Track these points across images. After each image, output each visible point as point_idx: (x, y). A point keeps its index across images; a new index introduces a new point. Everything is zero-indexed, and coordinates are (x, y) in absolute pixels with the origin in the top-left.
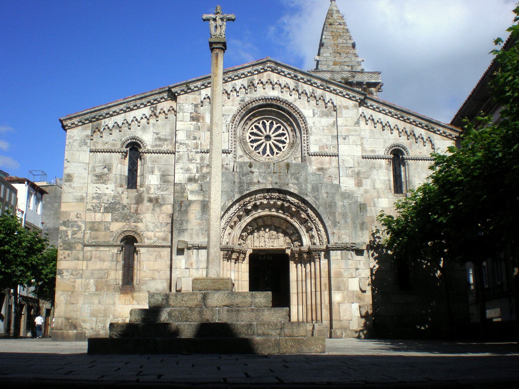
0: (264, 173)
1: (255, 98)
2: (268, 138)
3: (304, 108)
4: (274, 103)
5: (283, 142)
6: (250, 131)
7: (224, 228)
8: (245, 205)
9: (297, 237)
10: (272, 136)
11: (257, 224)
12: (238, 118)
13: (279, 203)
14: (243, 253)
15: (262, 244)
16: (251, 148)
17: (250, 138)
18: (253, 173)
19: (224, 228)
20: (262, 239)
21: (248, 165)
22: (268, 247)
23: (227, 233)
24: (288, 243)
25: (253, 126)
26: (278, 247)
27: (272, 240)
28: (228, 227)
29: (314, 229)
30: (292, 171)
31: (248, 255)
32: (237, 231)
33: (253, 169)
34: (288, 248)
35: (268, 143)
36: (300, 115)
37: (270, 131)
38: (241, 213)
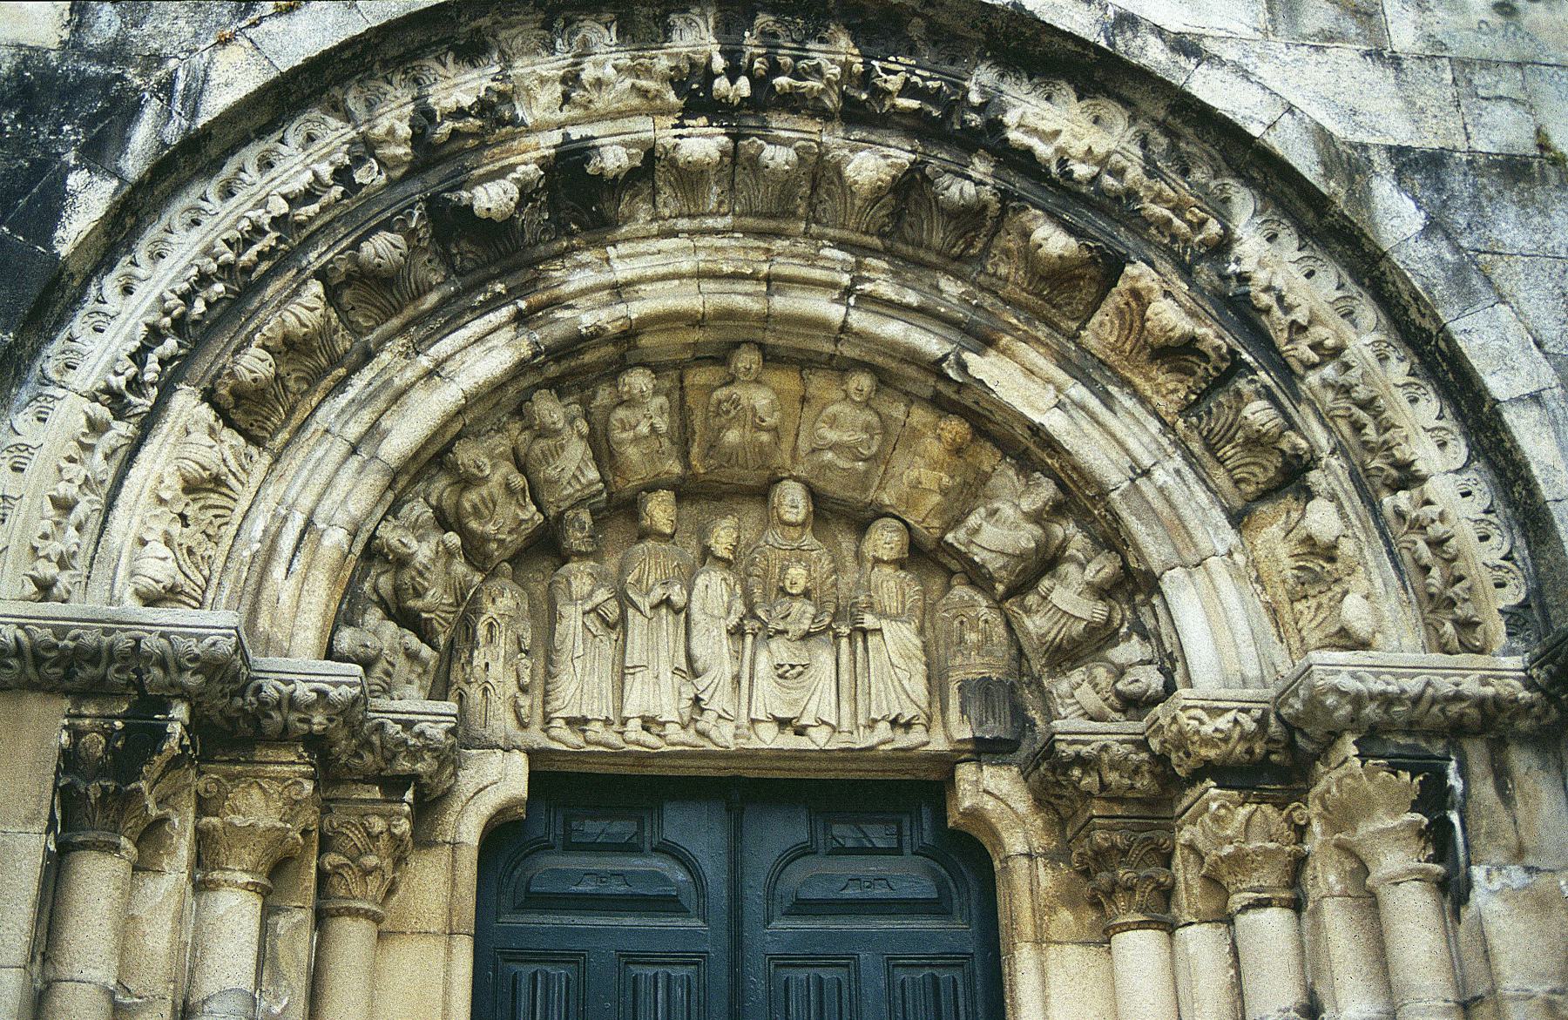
7: (116, 401)
8: (439, 153)
9: (1102, 592)
11: (602, 450)
13: (869, 164)
14: (393, 785)
15: (656, 694)
19: (116, 401)
20: (654, 642)
22: (725, 737)
23: (158, 465)
24: (981, 692)
26: (863, 740)
27: (781, 651)
28: (187, 404)
29: (1330, 475)
31: (467, 826)
32: (324, 484)
34: (985, 750)
38: (382, 247)
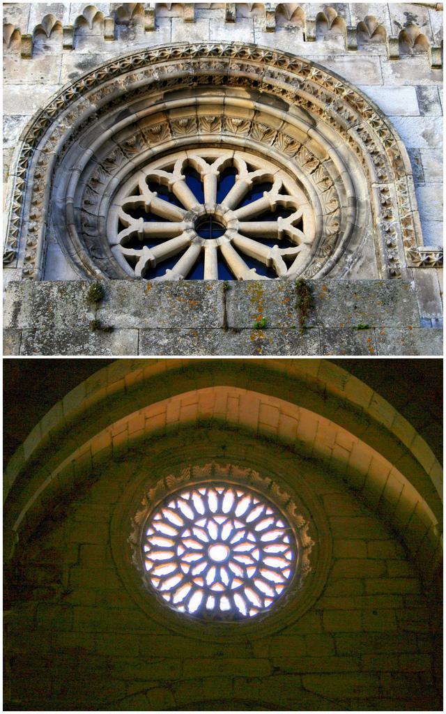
0: (171, 330)
1: (147, 52)
2: (209, 226)
3: (379, 80)
4: (235, 71)
5: (285, 240)
6: (125, 198)
10: (230, 217)
12: (62, 127)
16: (127, 267)
17: (122, 226)
18: (111, 330)
21: (80, 296)
25: (141, 180)
30: (329, 321)
33: (109, 315)
35: (210, 246)
36: (356, 107)
37: (219, 199)
